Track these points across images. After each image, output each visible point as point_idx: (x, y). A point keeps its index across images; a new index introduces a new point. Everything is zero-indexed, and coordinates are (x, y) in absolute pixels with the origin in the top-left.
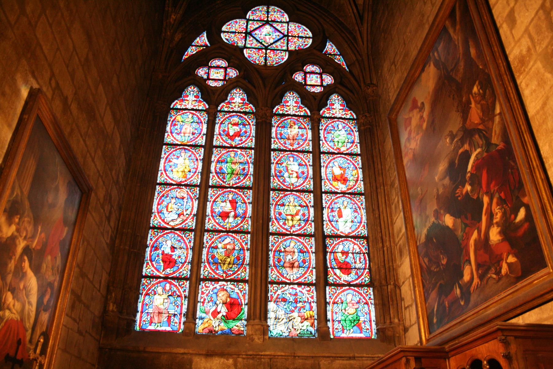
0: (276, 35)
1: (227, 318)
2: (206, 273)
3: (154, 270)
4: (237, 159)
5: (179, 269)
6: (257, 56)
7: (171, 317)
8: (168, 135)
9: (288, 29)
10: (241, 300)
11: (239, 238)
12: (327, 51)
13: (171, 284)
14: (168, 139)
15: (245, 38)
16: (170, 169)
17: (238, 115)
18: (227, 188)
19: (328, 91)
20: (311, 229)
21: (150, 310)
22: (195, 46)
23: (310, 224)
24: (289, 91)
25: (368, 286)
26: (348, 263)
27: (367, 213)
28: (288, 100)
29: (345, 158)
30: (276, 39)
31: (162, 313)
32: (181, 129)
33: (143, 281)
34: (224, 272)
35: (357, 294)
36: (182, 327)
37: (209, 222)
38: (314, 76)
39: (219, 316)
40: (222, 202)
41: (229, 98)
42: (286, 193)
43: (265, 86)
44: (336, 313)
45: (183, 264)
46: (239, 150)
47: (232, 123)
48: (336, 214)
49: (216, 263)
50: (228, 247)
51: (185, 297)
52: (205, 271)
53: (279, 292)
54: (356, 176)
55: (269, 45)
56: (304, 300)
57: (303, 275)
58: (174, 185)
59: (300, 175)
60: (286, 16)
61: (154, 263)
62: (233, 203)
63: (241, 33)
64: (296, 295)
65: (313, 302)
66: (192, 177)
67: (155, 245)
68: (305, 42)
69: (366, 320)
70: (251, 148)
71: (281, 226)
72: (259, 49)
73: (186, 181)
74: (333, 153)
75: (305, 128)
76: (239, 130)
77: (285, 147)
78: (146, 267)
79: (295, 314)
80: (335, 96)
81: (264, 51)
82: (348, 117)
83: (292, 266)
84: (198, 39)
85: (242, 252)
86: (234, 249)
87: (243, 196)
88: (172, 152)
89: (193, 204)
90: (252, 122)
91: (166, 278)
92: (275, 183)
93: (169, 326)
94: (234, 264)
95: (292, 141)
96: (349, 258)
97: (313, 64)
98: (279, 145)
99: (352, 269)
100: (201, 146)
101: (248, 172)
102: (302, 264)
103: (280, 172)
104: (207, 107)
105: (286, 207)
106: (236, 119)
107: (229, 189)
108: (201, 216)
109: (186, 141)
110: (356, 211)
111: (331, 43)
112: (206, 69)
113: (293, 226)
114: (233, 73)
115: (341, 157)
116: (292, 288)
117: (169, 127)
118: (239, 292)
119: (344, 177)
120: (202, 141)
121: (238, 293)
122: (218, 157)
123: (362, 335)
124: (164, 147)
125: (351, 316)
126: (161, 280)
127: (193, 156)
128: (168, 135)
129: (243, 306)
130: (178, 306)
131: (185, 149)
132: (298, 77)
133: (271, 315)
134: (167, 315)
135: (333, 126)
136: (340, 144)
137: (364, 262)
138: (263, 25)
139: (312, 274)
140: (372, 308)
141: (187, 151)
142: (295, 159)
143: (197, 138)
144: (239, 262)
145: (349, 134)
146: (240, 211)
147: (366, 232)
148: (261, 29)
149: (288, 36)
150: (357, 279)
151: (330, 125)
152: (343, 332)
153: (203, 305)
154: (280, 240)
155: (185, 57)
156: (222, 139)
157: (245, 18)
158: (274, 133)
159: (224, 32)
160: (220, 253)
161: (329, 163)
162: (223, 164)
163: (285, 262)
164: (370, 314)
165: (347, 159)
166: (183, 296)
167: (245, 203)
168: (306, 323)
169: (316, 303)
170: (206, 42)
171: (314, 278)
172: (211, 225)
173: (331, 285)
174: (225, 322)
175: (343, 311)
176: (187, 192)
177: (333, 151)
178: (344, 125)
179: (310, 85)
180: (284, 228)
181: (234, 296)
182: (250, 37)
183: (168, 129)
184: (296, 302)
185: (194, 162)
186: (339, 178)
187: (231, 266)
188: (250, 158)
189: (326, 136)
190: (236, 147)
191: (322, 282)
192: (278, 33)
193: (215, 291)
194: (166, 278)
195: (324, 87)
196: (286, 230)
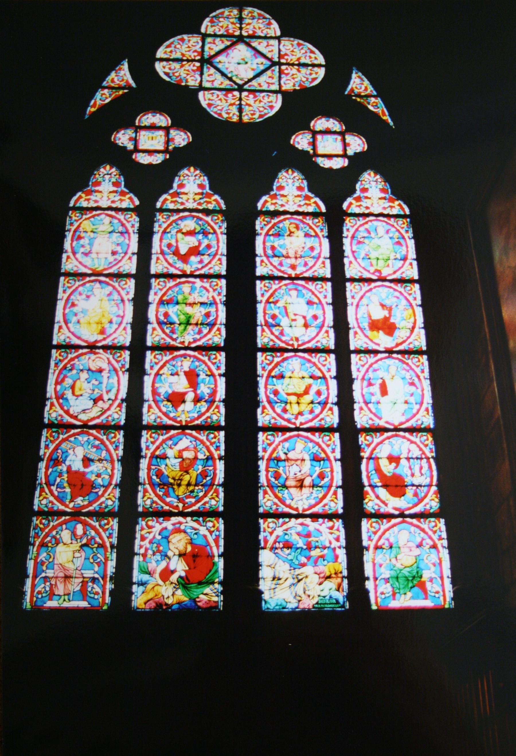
0: (260, 63)
2: (148, 502)
3: (55, 501)
4: (196, 297)
5: (99, 497)
6: (224, 104)
7: (87, 582)
9: (280, 51)
10: (211, 548)
12: (352, 90)
13: (85, 524)
14: (68, 264)
17: (194, 217)
18: (178, 349)
19: (358, 164)
20: (332, 418)
21: (50, 573)
22: (109, 88)
23: (331, 409)
25: (436, 515)
29: (390, 287)
30: (258, 71)
32: (91, 244)
33: (36, 521)
34: (180, 500)
36: (108, 600)
37: (149, 411)
38: (330, 138)
41: (175, 185)
45: (106, 487)
48: (376, 389)
49: (164, 484)
50: (186, 454)
51: (112, 546)
52: (145, 499)
53: (279, 532)
55: (246, 83)
56: (323, 544)
58: (82, 347)
60: (275, 25)
61: (54, 488)
63: (193, 60)
64: (308, 535)
65: (340, 547)
66: (115, 332)
67: (55, 456)
70: (219, 276)
71: (278, 415)
72: (228, 91)
74: (369, 281)
75: (317, 235)
76: (197, 244)
78: (40, 495)
79: (309, 570)
80: (369, 174)
83: (300, 485)
84: (113, 74)
85: (210, 463)
86: (196, 458)
87: (209, 364)
90: (220, 226)
92: (263, 338)
93: (84, 599)
94: (196, 485)
97: (328, 115)
99: (407, 486)
100: (128, 276)
102: (317, 481)
103: (274, 317)
104: (137, 203)
105: (286, 381)
106: (189, 224)
107: (182, 352)
111: (360, 74)
112: (130, 133)
113: (301, 413)
114: (181, 138)
115: (383, 286)
116: (302, 524)
118: (207, 533)
122: (160, 294)
126: (67, 517)
128: (68, 257)
130: (99, 564)
131: (100, 282)
132: (301, 141)
133: (265, 573)
136: (381, 263)
137: (428, 473)
138: (233, 44)
139: (336, 498)
140: (445, 555)
141: (104, 285)
143: (120, 261)
145: (398, 243)
146: (204, 390)
148: (230, 51)
150: (416, 505)
151: (362, 229)
152: (394, 599)
153: (144, 560)
155: (91, 110)
156: (166, 260)
157: (199, 32)
159: (161, 60)
160: (171, 467)
161: (362, 297)
162: (170, 306)
163: (287, 479)
165: (395, 290)
166: (108, 545)
167: (213, 375)
170: (127, 82)
175: (394, 560)
176: (108, 359)
181: (200, 541)
183: (67, 245)
184: (309, 547)
185: (117, 305)
186: (380, 325)
187: (191, 488)
188: (219, 294)
189: (354, 248)
190: (192, 275)
191: (353, 514)
193: (165, 533)
194: (76, 514)
195: (349, 158)
196: (288, 421)
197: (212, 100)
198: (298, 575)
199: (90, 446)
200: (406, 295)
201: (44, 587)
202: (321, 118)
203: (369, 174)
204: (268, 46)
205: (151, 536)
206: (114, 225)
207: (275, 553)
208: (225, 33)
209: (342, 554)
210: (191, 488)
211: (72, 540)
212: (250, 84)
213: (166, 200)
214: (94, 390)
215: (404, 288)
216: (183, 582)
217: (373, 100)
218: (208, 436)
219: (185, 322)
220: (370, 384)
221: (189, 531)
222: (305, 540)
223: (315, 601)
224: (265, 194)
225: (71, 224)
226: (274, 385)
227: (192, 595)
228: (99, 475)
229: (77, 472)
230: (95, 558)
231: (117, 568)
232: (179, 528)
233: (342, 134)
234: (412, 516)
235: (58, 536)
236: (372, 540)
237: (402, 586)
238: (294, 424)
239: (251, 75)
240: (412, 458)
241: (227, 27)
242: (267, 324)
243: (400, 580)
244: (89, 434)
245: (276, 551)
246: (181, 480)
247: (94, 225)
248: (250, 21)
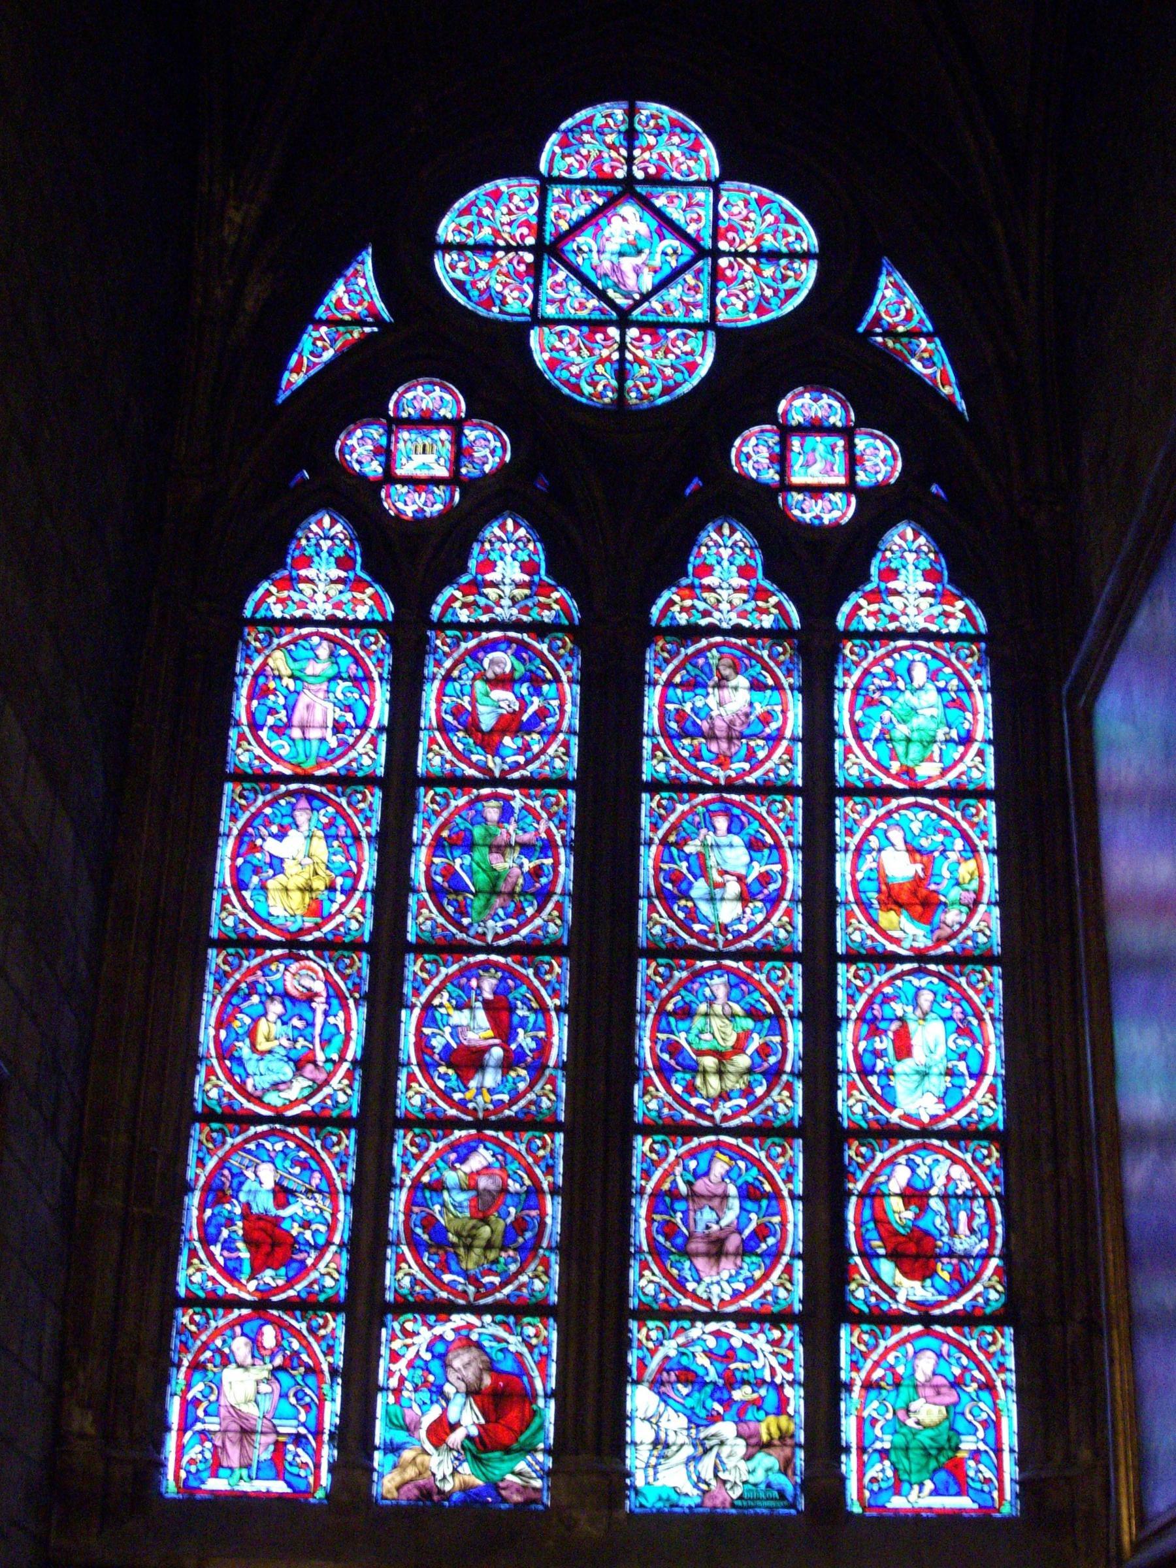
1: (480, 1447)
2: (406, 1282)
3: (219, 1278)
5: (304, 1270)
7: (285, 1444)
8: (242, 737)
9: (717, 217)
10: (531, 1379)
11: (523, 1148)
12: (877, 318)
13: (280, 1325)
15: (535, 271)
16: (255, 880)
17: (510, 641)
18: (472, 950)
19: (879, 509)
20: (789, 1105)
21: (212, 1424)
22: (332, 322)
23: (789, 1086)
24: (712, 519)
25: (997, 1320)
26: (927, 1233)
27: (1010, 1036)
28: (711, 560)
29: (933, 809)
30: (666, 271)
31: (254, 1432)
32: (290, 709)
33: (184, 1318)
35: (953, 1350)
36: (326, 1479)
37: (408, 1088)
38: (819, 443)
39: (456, 1438)
40: (459, 1007)
41: (472, 564)
42: (699, 964)
43: (617, 492)
44: (874, 1421)
45: (322, 1250)
46: (516, 792)
47: (490, 675)
48: (885, 1043)
50: (483, 1182)
51: (334, 1371)
52: (402, 1274)
53: (670, 1348)
54: (975, 885)
56: (759, 1375)
57: (757, 1284)
58: (273, 945)
59: (756, 888)
60: (709, 151)
62: (500, 1012)
63: (520, 248)
65: (791, 1384)
66: (340, 911)
68: (785, 278)
69: (982, 1447)
70: (562, 783)
73: (318, 927)
74: (887, 793)
75: (778, 687)
77: (696, 771)
78: (190, 1264)
79: (726, 1429)
81: (613, 332)
82: (954, 626)
83: (717, 1249)
84: (340, 288)
86: (504, 1190)
87: (537, 983)
88: (260, 811)
89: (347, 1022)
91: (261, 1306)
92: (652, 922)
93: (280, 1475)
94: (504, 1248)
95: (724, 745)
96: (929, 1216)
97: (818, 383)
98: (674, 762)
99: (938, 1257)
100: (370, 781)
101: (553, 882)
103: (676, 878)
104: (390, 608)
105: (698, 1022)
106: (503, 661)
107: (481, 957)
108: (378, 1065)
109: (311, 762)
110: (964, 1031)
111: (897, 276)
112: (375, 432)
113: (725, 1096)
117: (243, 701)
118: (524, 1350)
119: (923, 892)
120: (371, 757)
121: (518, 1356)
122: (437, 823)
123: (964, 1502)
124: (228, 787)
125: (930, 1433)
126: (245, 1311)
127: (340, 821)
128: (242, 737)
129: (541, 1402)
130: (307, 1407)
131: (311, 796)
134: (272, 1438)
135: (890, 674)
136: (915, 750)
137: (986, 1230)
138: (612, 202)
139: (791, 1281)
140: (1009, 1403)
141: (316, 803)
142: (736, 823)
143: (353, 746)
144: (521, 1240)
146: (525, 1040)
147: (1000, 1115)
148: (603, 222)
149: (716, 253)
153: (398, 1401)
154: (673, 1153)
157: (534, 173)
158: (656, 712)
159: (448, 247)
162: (457, 853)
164: (997, 1426)
166: (325, 1367)
167: (543, 1009)
168: (766, 1461)
169: (805, 1385)
170: (371, 308)
171: (799, 1291)
172: (417, 1101)
173: (856, 1319)
174: (477, 1459)
177: (887, 781)
178: (935, 664)
179: (801, 489)
180: (688, 1107)
181: (508, 1365)
182: (555, 270)
184: (731, 1381)
185: (346, 848)
186: (904, 897)
187: (492, 1255)
189: (858, 715)
190: (504, 781)
191: (825, 1313)
192: (671, 242)
193: (440, 1348)
196: (699, 1111)
197: (558, 350)
198: (706, 1438)
199: (288, 1163)
200: (965, 825)
201: (202, 1452)
202: (801, 395)
203: (902, 536)
204: (689, 205)
205: (410, 1354)
206: (340, 660)
207: (659, 1394)
208: (593, 175)
209: (796, 1397)
210: (492, 1255)
211: (253, 1357)
212: (646, 305)
213: (453, 599)
214: (295, 1041)
215: (963, 810)
216: (472, 1447)
217: (923, 342)
218: (529, 1142)
219: (487, 889)
220: (875, 1032)
221: (486, 1344)
222: (720, 1367)
223: (735, 1494)
224: (667, 585)
225: (249, 659)
226: (672, 1032)
227: (490, 1475)
228: (306, 1225)
229: (263, 1217)
230: (300, 1395)
231: (343, 1416)
232: (468, 1337)
233: (847, 433)
234: (944, 1320)
235: (226, 1350)
236: (858, 1370)
237: (914, 1467)
238: (711, 1118)
239: (648, 282)
240: (957, 1196)
241: (600, 157)
242: (662, 893)
243: (911, 1455)
244: (286, 1136)
245: (663, 1389)
246: (474, 1237)
247: (295, 660)
248: (652, 140)
